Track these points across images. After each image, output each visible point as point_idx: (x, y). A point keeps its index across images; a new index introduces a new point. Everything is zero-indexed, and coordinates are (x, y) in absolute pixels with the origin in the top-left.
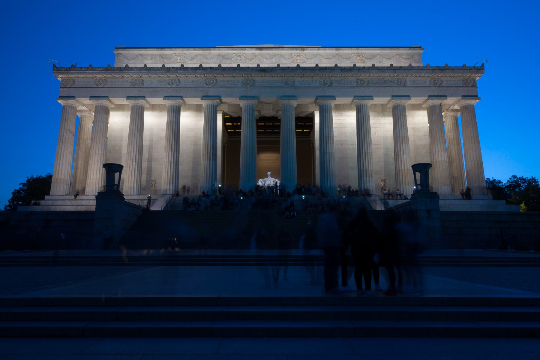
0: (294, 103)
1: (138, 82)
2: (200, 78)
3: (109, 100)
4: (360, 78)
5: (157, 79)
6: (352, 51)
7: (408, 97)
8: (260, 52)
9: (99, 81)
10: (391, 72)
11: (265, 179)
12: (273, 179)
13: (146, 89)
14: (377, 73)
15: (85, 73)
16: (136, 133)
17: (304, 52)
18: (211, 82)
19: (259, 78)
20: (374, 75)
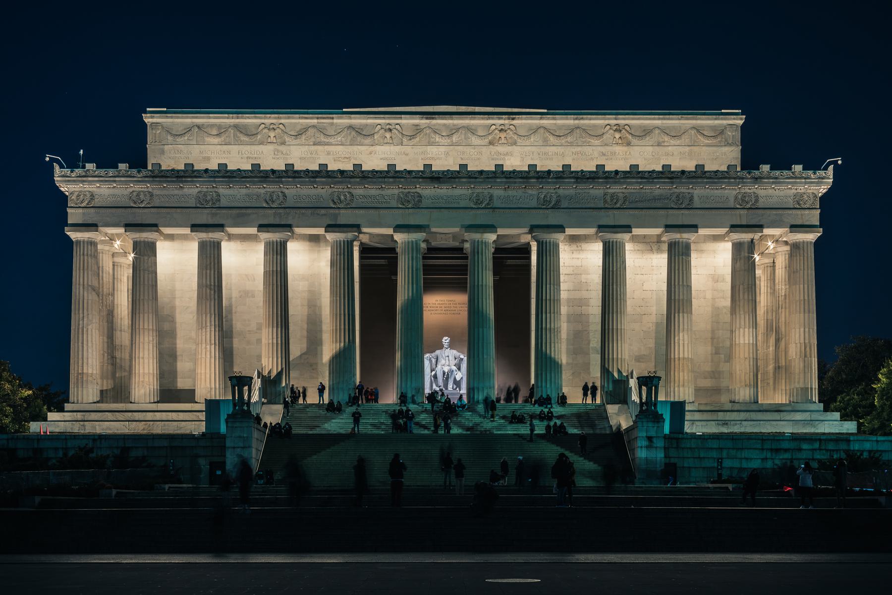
0: (491, 237)
1: (209, 198)
2: (321, 191)
3: (158, 231)
4: (610, 191)
5: (244, 191)
6: (607, 122)
7: (694, 227)
8: (428, 121)
9: (138, 195)
10: (664, 183)
11: (438, 352)
12: (455, 352)
13: (224, 211)
14: (641, 183)
15: (115, 181)
16: (212, 292)
17: (514, 122)
18: (342, 197)
19: (428, 191)
20: (633, 188)
